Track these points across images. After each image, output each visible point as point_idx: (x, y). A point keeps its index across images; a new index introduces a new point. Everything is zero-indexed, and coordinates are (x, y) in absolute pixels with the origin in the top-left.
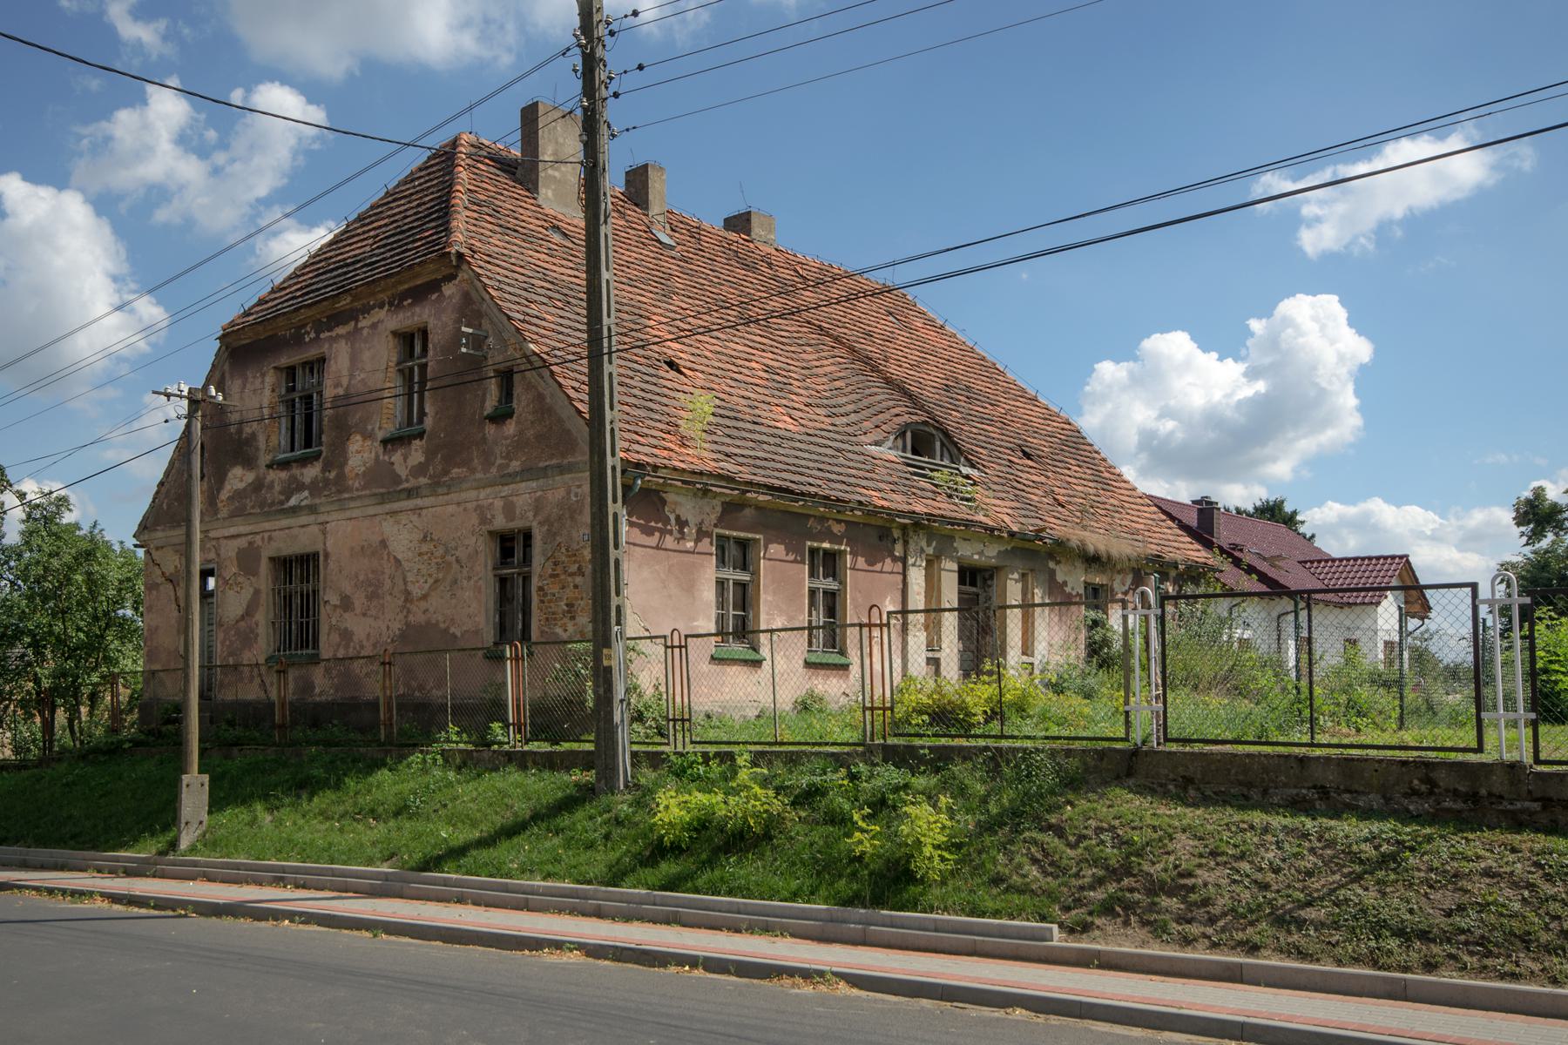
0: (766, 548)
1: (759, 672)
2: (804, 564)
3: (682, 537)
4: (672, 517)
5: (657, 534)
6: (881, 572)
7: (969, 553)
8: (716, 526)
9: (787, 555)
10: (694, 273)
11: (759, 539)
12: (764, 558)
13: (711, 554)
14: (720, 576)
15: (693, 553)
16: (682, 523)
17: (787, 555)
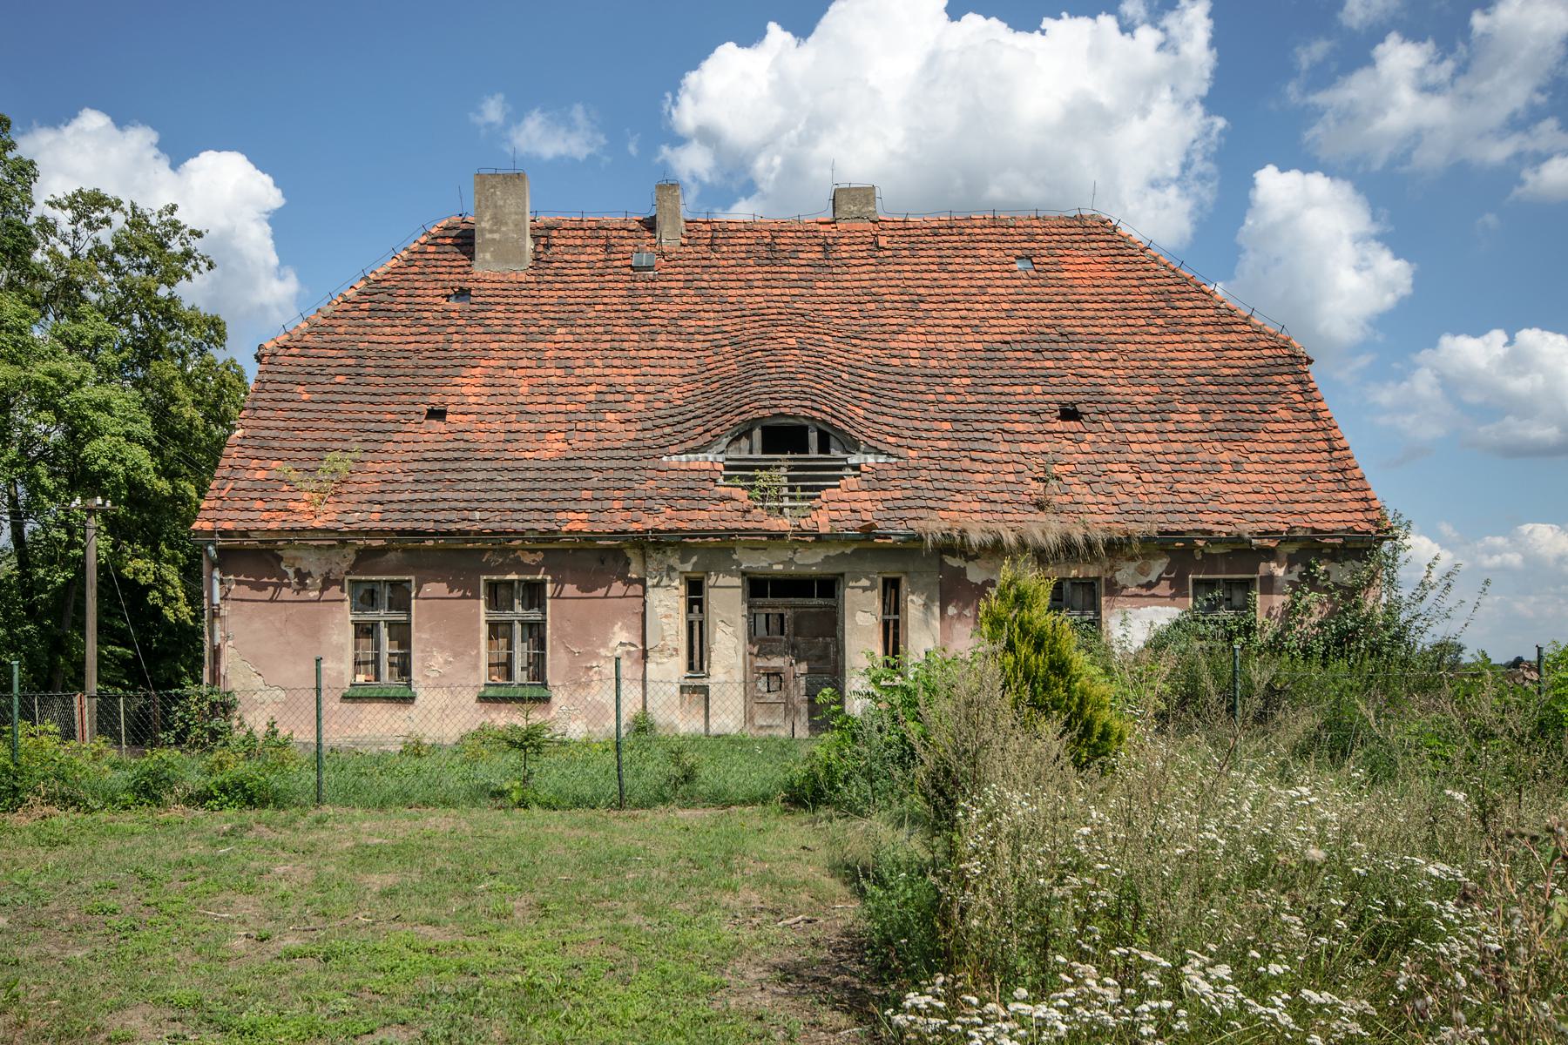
0: (419, 589)
1: (411, 707)
2: (479, 598)
3: (303, 586)
4: (291, 572)
5: (271, 589)
6: (606, 597)
7: (765, 564)
8: (348, 573)
9: (451, 591)
10: (941, 306)
11: (410, 581)
12: (416, 597)
13: (342, 601)
14: (363, 618)
15: (318, 601)
16: (302, 576)
17: (451, 591)
